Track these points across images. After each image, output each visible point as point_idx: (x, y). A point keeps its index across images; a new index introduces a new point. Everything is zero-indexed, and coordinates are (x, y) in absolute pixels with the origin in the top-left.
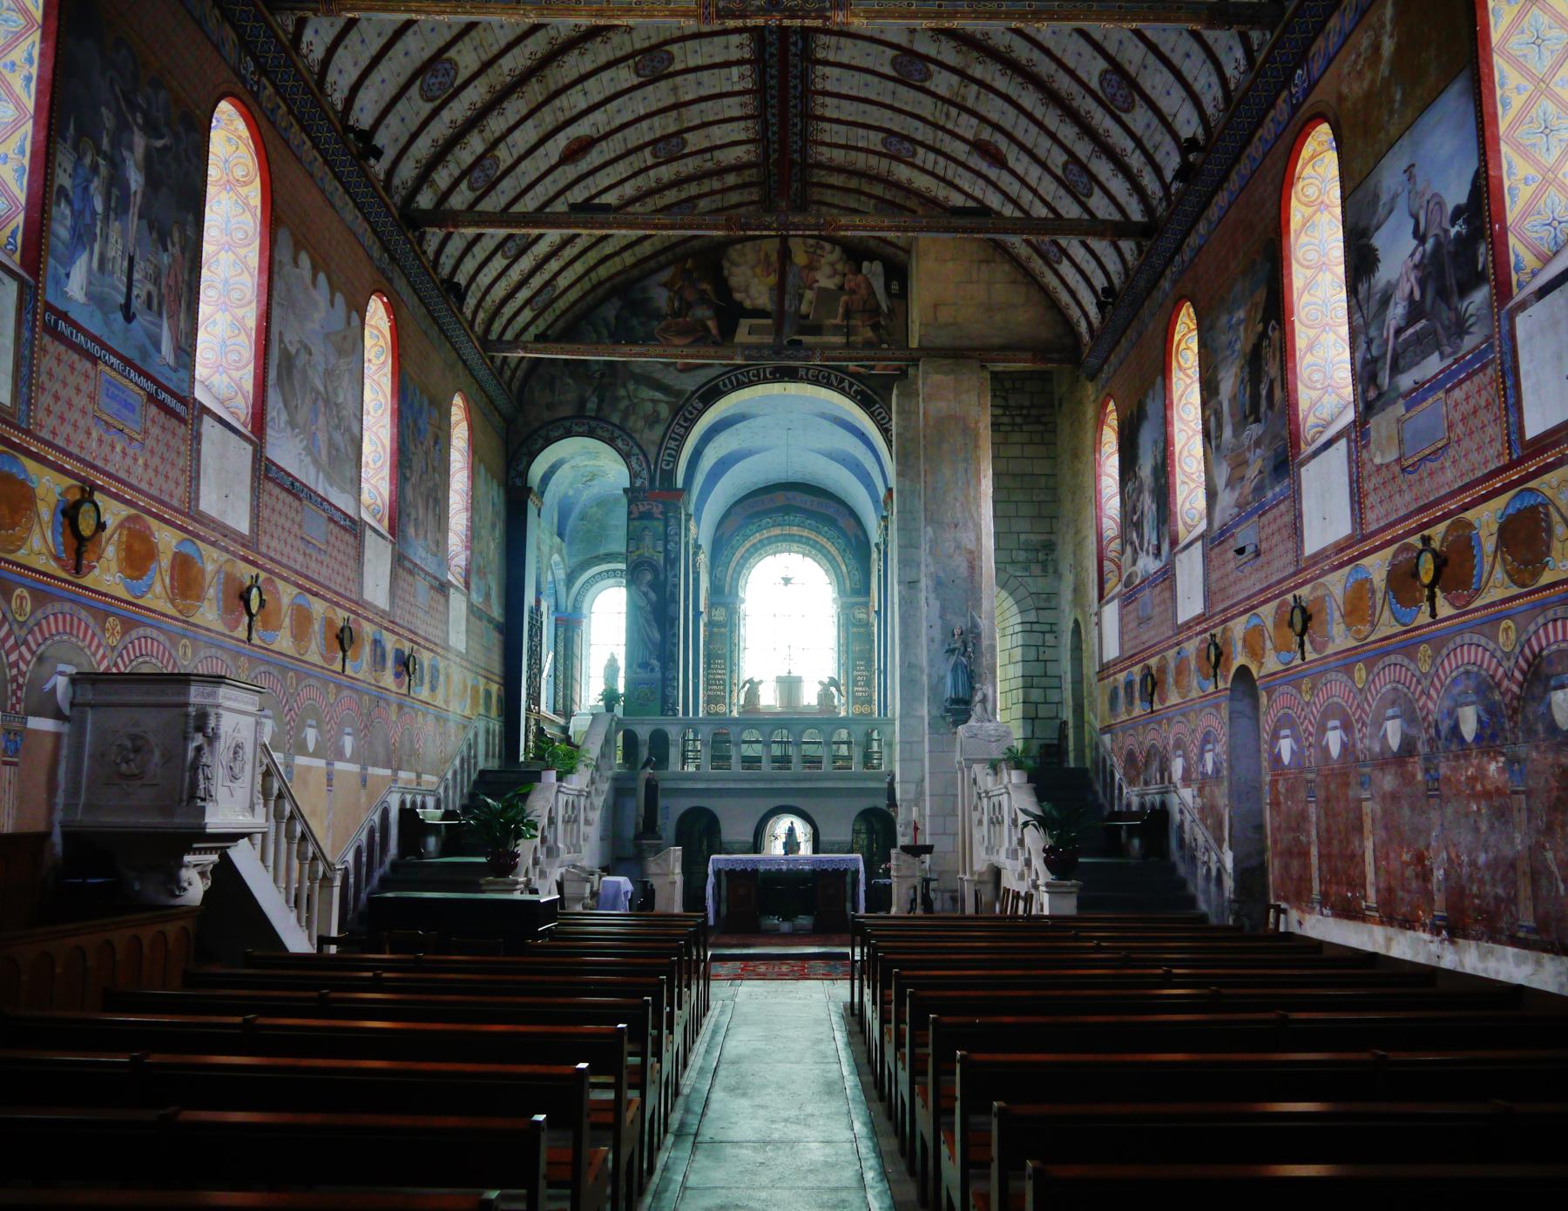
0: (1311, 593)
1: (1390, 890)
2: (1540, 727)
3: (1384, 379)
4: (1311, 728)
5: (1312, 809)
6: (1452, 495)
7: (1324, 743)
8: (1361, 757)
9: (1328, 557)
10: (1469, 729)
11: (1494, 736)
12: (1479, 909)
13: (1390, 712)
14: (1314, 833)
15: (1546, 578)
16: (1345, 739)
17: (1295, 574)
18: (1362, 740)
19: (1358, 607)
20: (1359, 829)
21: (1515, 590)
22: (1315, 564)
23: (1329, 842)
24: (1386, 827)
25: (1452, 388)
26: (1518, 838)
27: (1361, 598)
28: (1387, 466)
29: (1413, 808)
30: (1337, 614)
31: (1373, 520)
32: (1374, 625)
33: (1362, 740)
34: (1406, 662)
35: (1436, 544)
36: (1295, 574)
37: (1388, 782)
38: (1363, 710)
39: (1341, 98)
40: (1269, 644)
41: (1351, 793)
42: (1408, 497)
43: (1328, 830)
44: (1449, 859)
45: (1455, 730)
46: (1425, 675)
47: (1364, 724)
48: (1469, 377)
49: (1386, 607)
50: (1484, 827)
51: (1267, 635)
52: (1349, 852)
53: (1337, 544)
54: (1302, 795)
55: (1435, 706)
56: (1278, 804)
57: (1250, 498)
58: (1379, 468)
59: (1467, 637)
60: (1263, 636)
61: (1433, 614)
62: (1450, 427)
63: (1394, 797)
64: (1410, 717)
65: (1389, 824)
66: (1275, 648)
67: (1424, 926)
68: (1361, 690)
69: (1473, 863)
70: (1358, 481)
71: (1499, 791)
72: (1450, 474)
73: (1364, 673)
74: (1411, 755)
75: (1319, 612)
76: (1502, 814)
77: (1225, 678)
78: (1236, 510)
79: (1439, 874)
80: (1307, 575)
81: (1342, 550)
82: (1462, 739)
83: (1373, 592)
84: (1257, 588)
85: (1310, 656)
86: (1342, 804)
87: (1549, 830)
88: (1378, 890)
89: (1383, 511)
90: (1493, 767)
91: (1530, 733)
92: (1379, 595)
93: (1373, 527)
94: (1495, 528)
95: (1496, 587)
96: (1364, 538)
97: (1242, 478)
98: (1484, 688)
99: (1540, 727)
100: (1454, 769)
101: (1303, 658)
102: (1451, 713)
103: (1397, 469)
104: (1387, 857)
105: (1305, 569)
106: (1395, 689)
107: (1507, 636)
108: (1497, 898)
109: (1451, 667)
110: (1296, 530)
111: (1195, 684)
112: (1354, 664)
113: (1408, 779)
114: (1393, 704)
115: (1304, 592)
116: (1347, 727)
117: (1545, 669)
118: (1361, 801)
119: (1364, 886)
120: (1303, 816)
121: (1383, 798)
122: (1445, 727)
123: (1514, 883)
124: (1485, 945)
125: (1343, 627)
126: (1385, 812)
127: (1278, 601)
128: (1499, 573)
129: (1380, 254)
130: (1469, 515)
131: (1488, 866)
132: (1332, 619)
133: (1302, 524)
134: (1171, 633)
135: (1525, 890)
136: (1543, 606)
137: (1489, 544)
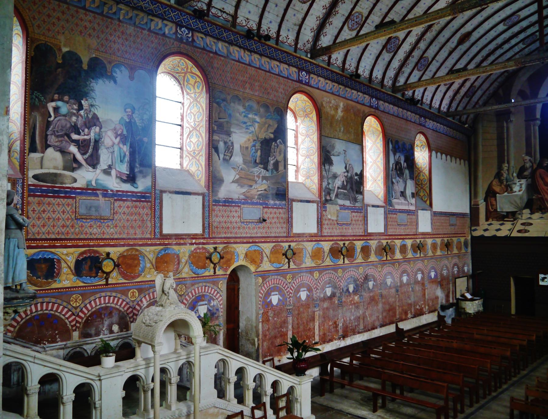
0: (296, 245)
1: (324, 334)
2: (367, 289)
3: (333, 196)
4: (291, 291)
5: (290, 319)
6: (351, 236)
7: (298, 296)
8: (316, 299)
9: (306, 237)
10: (351, 290)
11: (357, 291)
12: (351, 330)
13: (328, 286)
14: (290, 327)
15: (369, 260)
16: (309, 294)
17: (286, 237)
18: (316, 294)
19: (317, 254)
20: (313, 319)
21: (363, 261)
22: (299, 237)
23: (299, 327)
24: (324, 318)
25: (355, 212)
26: (361, 312)
27: (319, 253)
28: (333, 220)
29: (333, 310)
30: (308, 255)
31: (326, 232)
32: (323, 262)
33: (316, 294)
34: (334, 273)
35: (346, 245)
36: (286, 237)
37: (326, 305)
38: (317, 285)
39: (322, 104)
40: (265, 259)
41: (310, 310)
42: (338, 231)
43: (298, 324)
44: (344, 321)
45: (348, 290)
46: (340, 277)
47: (317, 289)
48: (358, 212)
49: (328, 257)
50: (353, 311)
51: (264, 255)
52: (308, 328)
53: (310, 234)
54: (284, 314)
55: (343, 284)
56: (268, 320)
57: (256, 197)
58: (329, 220)
59: (352, 269)
60: (262, 255)
61: (344, 262)
62: (352, 220)
63: (327, 309)
64: (334, 287)
65: (325, 317)
66: (270, 261)
67: (336, 339)
68: (316, 280)
69: (350, 320)
70: (321, 219)
71: (357, 302)
72: (350, 231)
73: (318, 275)
74: (334, 296)
75: (299, 253)
76: (357, 307)
77: (226, 270)
78: (242, 197)
79: (341, 325)
80: (290, 239)
81: (312, 236)
82: (349, 292)
83: (324, 252)
84: (259, 235)
85: (292, 266)
86: (305, 314)
87: (367, 308)
88: (320, 336)
89: (330, 231)
90: (356, 298)
91: (365, 290)
92: (326, 254)
93: (326, 234)
94: (360, 247)
95: (359, 259)
96: (322, 236)
97: (251, 186)
98: (355, 281)
99: (367, 289)
100: (347, 299)
101: (289, 267)
102: (347, 286)
103: (336, 223)
104: (324, 325)
105: (290, 237)
106: (330, 280)
107: (361, 270)
108: (356, 326)
109: (347, 275)
110: (289, 221)
111: (186, 269)
112: (314, 272)
113: (332, 303)
114: (329, 283)
115: (293, 245)
116: (310, 290)
117: (368, 278)
118: (314, 312)
119: (314, 337)
120: (285, 322)
121: (324, 309)
122: (345, 289)
123: (359, 321)
124: (352, 337)
125: (310, 260)
126: (324, 313)
127: (274, 244)
128: (360, 257)
129: (334, 163)
130: (355, 242)
131: (354, 319)
132: (306, 257)
133: (292, 221)
134: (148, 236)
135: (361, 321)
136: (369, 265)
137: (359, 250)
